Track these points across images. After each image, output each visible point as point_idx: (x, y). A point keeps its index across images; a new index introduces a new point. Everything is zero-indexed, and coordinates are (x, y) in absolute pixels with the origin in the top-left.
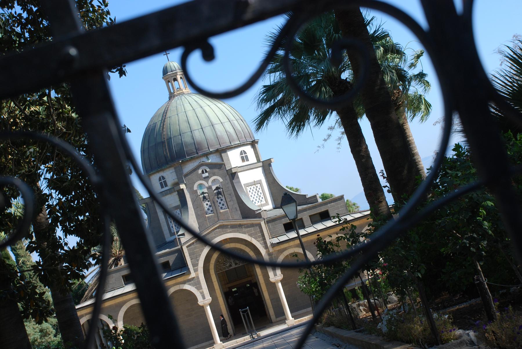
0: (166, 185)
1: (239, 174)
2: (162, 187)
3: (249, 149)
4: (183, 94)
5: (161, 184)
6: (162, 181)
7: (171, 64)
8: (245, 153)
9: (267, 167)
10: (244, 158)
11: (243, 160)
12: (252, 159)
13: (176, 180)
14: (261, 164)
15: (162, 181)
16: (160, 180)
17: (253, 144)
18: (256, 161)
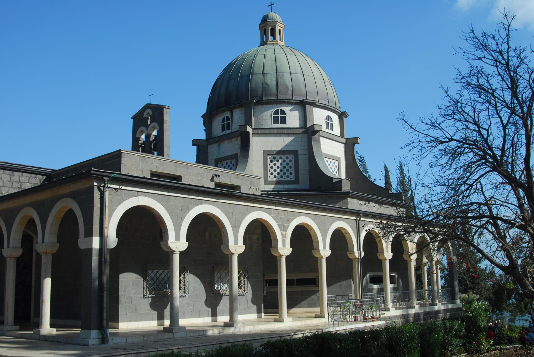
0: (229, 128)
1: (322, 139)
2: (223, 130)
3: (335, 118)
4: (277, 44)
5: (223, 126)
6: (226, 122)
7: (274, 14)
8: (331, 120)
9: (350, 145)
10: (329, 126)
11: (327, 127)
12: (337, 131)
13: (244, 124)
14: (344, 141)
15: (226, 122)
16: (223, 121)
17: (342, 116)
18: (339, 135)
